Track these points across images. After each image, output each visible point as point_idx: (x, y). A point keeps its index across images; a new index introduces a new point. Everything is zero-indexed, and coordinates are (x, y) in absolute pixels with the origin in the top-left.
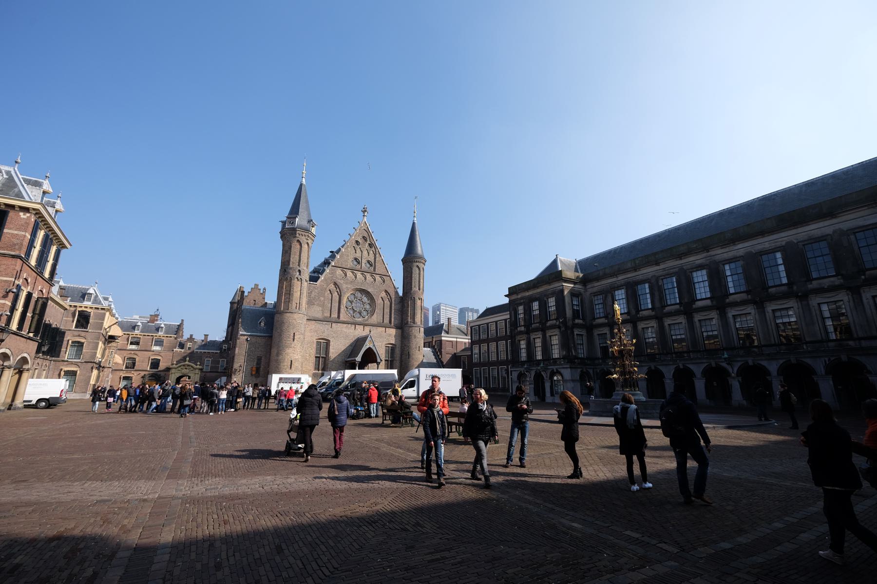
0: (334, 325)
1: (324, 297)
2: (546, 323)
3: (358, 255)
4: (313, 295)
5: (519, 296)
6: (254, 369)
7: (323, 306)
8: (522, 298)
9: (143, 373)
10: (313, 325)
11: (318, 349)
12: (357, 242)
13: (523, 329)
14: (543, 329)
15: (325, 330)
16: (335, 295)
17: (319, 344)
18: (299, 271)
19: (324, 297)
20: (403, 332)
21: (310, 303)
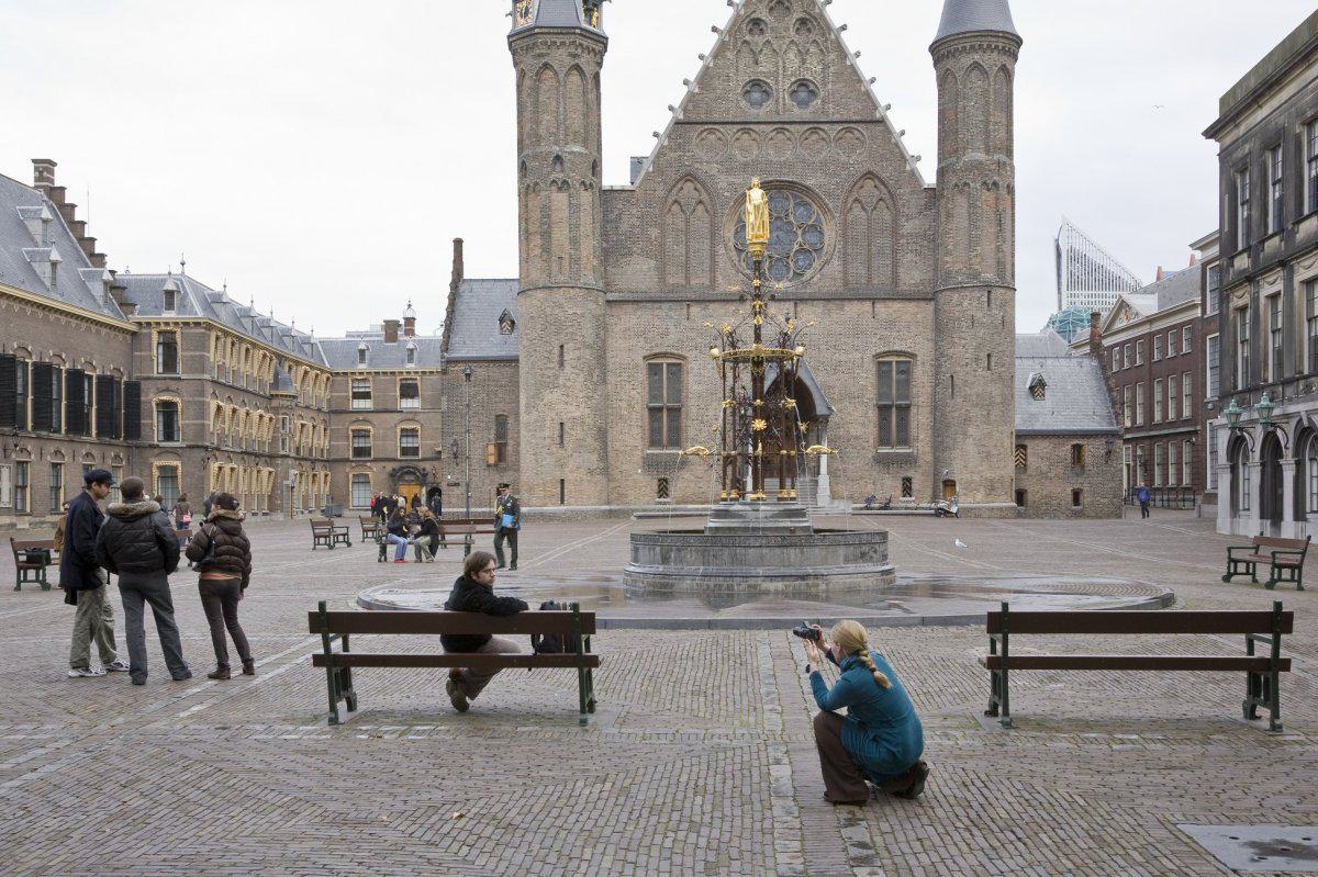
0: (695, 309)
1: (662, 227)
2: (1294, 233)
3: (765, 66)
4: (624, 227)
5: (1242, 129)
6: (492, 449)
7: (661, 256)
8: (1245, 138)
9: (390, 466)
10: (629, 320)
11: (654, 392)
12: (757, 22)
13: (1243, 262)
14: (1285, 263)
15: (670, 329)
16: (701, 219)
17: (654, 370)
18: (558, 158)
19: (662, 227)
20: (936, 311)
21: (611, 252)
